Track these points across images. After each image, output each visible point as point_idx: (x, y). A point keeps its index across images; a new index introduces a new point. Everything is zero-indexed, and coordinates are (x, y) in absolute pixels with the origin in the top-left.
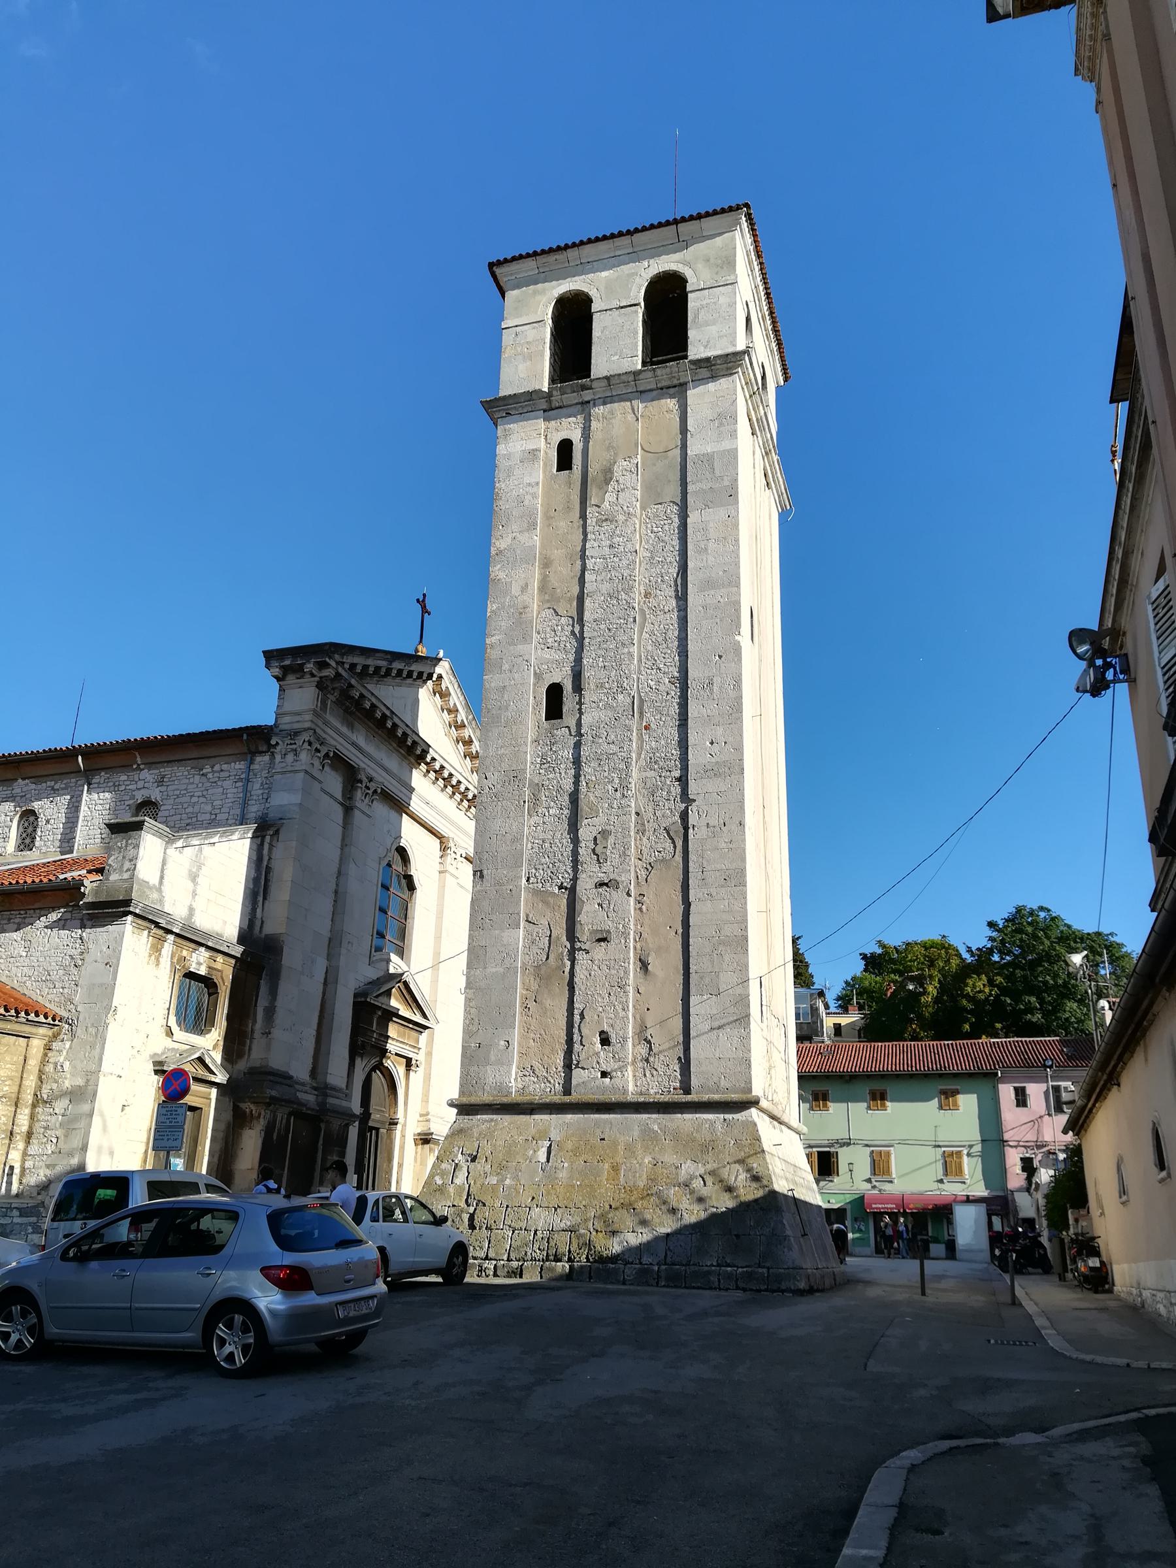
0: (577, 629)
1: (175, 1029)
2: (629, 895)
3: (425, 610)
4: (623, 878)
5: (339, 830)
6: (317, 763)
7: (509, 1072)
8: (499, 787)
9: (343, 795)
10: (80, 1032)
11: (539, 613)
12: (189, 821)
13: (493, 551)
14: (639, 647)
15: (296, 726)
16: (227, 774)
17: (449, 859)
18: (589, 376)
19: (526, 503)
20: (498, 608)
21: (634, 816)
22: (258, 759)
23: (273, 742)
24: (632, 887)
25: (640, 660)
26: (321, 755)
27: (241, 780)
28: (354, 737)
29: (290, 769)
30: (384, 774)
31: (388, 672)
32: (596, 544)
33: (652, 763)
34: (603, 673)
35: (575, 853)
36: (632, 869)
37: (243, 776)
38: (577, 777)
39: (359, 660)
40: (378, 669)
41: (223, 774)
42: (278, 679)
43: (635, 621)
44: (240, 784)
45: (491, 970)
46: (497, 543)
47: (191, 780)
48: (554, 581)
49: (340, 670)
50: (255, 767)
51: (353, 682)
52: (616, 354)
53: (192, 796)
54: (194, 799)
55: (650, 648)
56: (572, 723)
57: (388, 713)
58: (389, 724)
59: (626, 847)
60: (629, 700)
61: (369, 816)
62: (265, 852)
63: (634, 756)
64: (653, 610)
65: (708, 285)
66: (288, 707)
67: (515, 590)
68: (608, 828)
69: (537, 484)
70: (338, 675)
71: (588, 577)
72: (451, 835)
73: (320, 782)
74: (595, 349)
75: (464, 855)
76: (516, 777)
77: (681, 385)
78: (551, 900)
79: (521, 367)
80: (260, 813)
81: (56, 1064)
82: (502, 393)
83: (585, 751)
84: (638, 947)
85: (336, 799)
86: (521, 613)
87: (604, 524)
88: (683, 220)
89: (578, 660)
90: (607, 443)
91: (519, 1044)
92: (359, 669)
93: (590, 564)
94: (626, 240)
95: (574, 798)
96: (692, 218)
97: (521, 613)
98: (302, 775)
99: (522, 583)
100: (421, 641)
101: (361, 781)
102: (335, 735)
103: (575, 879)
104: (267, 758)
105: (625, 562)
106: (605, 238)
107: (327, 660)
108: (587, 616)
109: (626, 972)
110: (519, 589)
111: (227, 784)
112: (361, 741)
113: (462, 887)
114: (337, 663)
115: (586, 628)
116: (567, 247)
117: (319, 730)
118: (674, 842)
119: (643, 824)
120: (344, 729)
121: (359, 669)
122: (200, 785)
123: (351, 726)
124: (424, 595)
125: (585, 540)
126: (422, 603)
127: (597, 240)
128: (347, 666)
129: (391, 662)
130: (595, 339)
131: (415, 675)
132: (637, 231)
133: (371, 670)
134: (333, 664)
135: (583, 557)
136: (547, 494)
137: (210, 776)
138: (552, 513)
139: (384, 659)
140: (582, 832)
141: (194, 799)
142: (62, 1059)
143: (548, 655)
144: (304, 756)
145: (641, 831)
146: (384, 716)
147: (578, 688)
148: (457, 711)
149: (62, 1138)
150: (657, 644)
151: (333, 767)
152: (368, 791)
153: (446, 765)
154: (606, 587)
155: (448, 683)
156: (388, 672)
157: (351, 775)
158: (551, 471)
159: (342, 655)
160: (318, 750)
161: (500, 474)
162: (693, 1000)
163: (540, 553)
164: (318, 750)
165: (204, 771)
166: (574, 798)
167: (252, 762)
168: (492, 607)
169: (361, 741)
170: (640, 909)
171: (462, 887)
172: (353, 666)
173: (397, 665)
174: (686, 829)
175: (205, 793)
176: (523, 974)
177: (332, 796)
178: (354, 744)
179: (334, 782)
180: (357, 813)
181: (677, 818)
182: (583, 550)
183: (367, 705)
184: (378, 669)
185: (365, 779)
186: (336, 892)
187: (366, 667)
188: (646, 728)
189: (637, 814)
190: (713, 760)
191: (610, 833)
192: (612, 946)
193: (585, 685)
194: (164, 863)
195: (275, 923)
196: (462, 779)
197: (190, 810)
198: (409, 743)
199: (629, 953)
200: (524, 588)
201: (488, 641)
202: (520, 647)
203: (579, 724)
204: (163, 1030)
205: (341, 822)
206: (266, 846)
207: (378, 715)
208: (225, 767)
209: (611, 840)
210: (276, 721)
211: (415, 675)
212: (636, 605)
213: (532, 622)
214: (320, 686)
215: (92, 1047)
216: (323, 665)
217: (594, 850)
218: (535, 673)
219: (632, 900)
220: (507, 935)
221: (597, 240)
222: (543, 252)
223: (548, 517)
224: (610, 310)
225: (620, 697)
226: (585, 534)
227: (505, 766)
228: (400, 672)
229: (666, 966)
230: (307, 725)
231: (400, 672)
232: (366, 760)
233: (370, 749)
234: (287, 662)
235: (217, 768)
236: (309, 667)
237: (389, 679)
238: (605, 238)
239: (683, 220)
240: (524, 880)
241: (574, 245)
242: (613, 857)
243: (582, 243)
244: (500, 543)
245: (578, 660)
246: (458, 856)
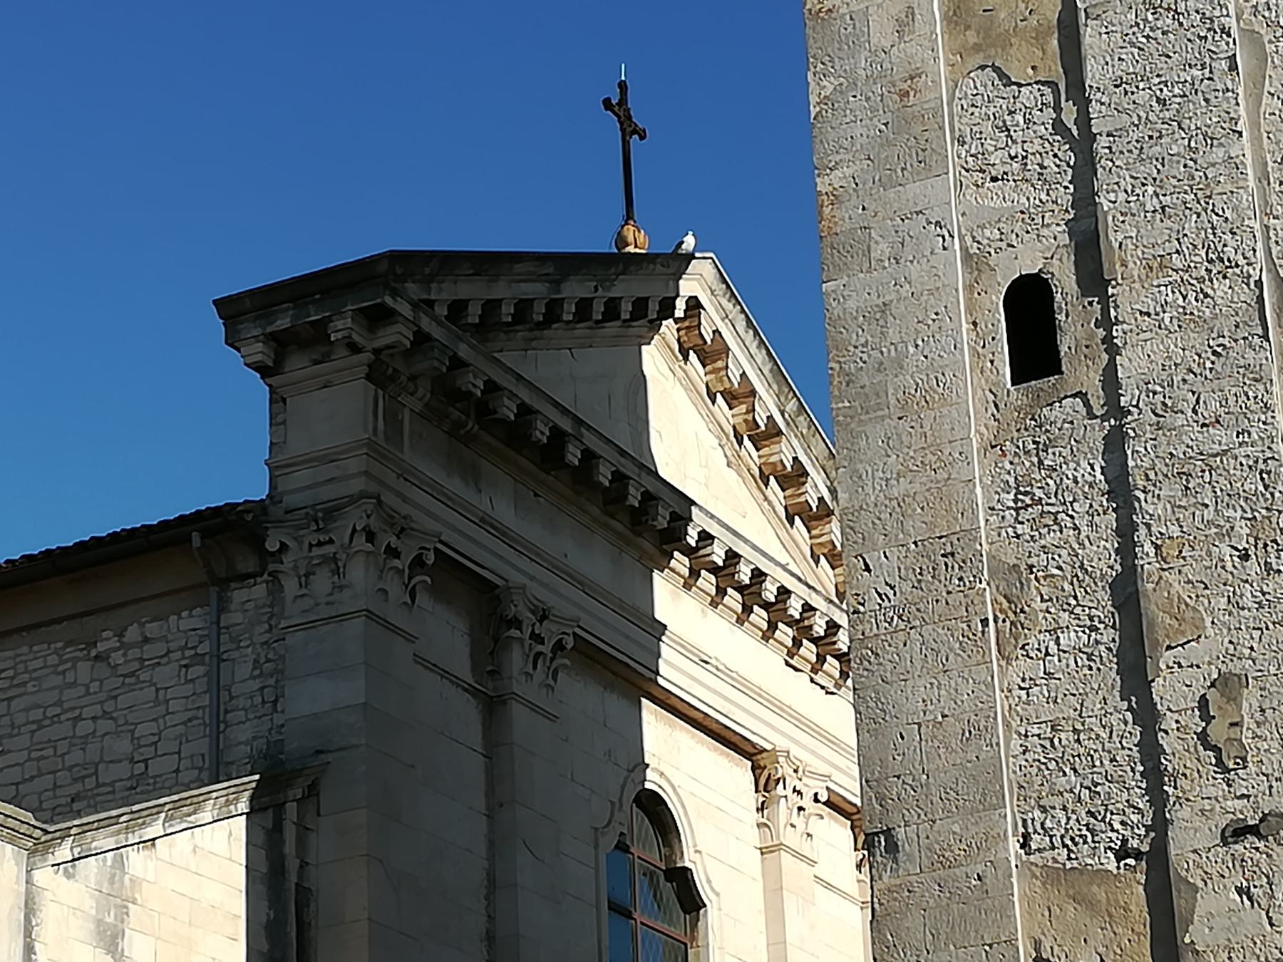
0: (1070, 115)
3: (629, 129)
6: (396, 589)
8: (907, 587)
9: (475, 667)
12: (78, 787)
14: (1256, 140)
15: (326, 493)
16: (160, 648)
17: (783, 811)
20: (838, 89)
22: (238, 596)
23: (272, 545)
25: (1264, 177)
26: (402, 563)
27: (198, 659)
28: (482, 502)
29: (325, 612)
30: (577, 595)
31: (553, 311)
34: (1161, 230)
35: (1150, 751)
37: (204, 648)
39: (473, 290)
40: (524, 306)
41: (150, 650)
42: (264, 371)
43: (1233, 67)
44: (198, 670)
47: (70, 677)
49: (426, 324)
50: (233, 617)
51: (464, 351)
53: (78, 719)
54: (84, 727)
56: (1092, 381)
57: (566, 425)
58: (573, 456)
60: (1247, 294)
61: (552, 718)
62: (290, 847)
66: (298, 445)
67: (881, 32)
68: (1235, 667)
70: (422, 338)
72: (781, 743)
73: (410, 638)
75: (823, 797)
78: (1100, 893)
80: (261, 744)
83: (1138, 458)
85: (456, 681)
89: (1085, 200)
92: (474, 314)
98: (359, 622)
99: (897, 9)
100: (629, 216)
101: (516, 623)
102: (438, 508)
103: (1160, 826)
104: (259, 591)
107: (388, 300)
108: (1093, 73)
110: (891, 26)
111: (165, 674)
112: (504, 512)
113: (829, 886)
114: (415, 305)
117: (388, 498)
120: (455, 485)
121: (474, 314)
122: (94, 686)
123: (473, 476)
124: (622, 86)
126: (619, 107)
128: (442, 311)
129: (556, 283)
131: (626, 309)
133: (507, 312)
134: (404, 308)
137: (117, 658)
139: (539, 278)
141: (84, 727)
143: (995, 199)
144: (357, 572)
146: (558, 436)
148: (753, 393)
151: (436, 591)
152: (540, 648)
153: (741, 549)
156: (553, 311)
159: (427, 282)
160: (393, 552)
164: (393, 552)
165: (101, 647)
167: (222, 609)
168: (819, 88)
169: (504, 512)
171: (829, 886)
172: (458, 308)
173: (575, 289)
175: (109, 707)
177: (445, 674)
178: (486, 522)
180: (517, 710)
183: (509, 410)
184: (524, 306)
185: (528, 617)
186: (490, 938)
187: (492, 306)
191: (1242, 680)
194: (30, 908)
196: (790, 583)
197: (76, 757)
198: (634, 500)
200: (906, 22)
201: (822, 185)
202: (913, 189)
203: (1111, 381)
205: (476, 739)
206: (290, 832)
207: (541, 433)
208: (153, 629)
209: (1250, 699)
210: (272, 486)
211: (626, 309)
212: (1232, 23)
213: (938, 112)
214: (378, 375)
216: (378, 317)
217: (1203, 736)
218: (967, 256)
225: (1221, 289)
227: (915, 528)
228: (584, 307)
230: (356, 486)
231: (584, 307)
232: (523, 563)
233: (531, 531)
234: (283, 323)
235: (132, 634)
236: (341, 327)
237: (556, 331)
240: (1014, 845)
245: (1085, 200)
246: (807, 802)
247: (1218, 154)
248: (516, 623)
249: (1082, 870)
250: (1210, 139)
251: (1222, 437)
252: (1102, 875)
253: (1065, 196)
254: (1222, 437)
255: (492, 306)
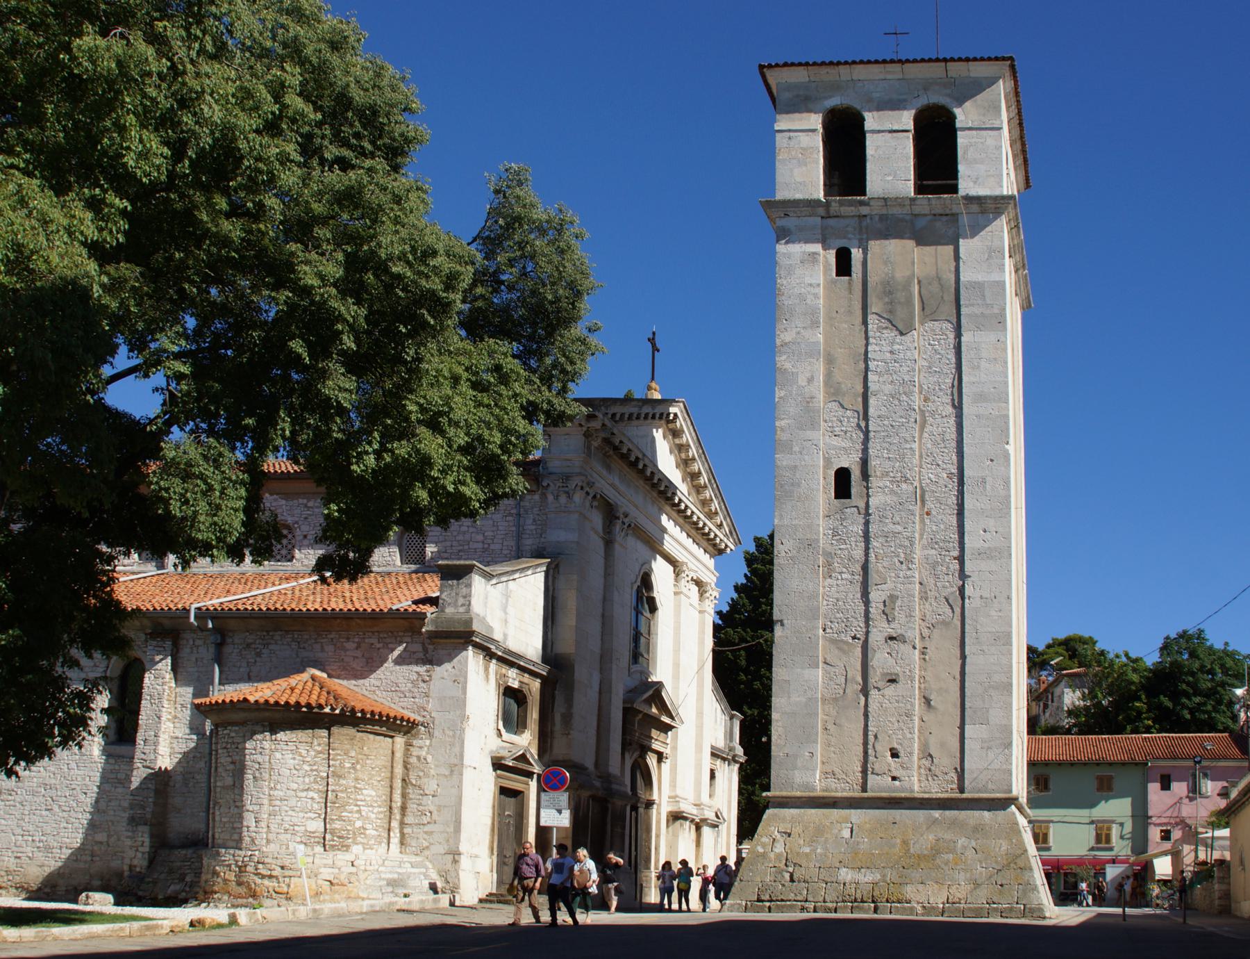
0: (863, 424)
1: (503, 731)
2: (914, 648)
4: (909, 634)
5: (602, 561)
7: (815, 775)
9: (604, 529)
10: (436, 733)
11: (825, 403)
13: (778, 342)
18: (863, 192)
19: (808, 301)
20: (785, 395)
21: (917, 586)
24: (917, 641)
25: (921, 456)
32: (877, 348)
33: (933, 543)
34: (887, 464)
35: (867, 613)
36: (917, 627)
38: (867, 549)
39: (618, 409)
45: (795, 698)
46: (782, 336)
48: (838, 376)
52: (890, 175)
55: (929, 446)
56: (862, 505)
57: (640, 456)
58: (641, 466)
59: (911, 609)
60: (911, 488)
63: (917, 535)
64: (933, 414)
65: (976, 125)
67: (802, 381)
68: (895, 593)
69: (819, 285)
71: (871, 376)
74: (870, 166)
76: (811, 544)
77: (953, 215)
78: (846, 647)
79: (796, 172)
81: (419, 758)
82: (780, 196)
83: (873, 528)
84: (923, 686)
86: (808, 402)
87: (885, 331)
88: (952, 60)
89: (865, 450)
90: (885, 257)
91: (822, 755)
93: (872, 365)
94: (897, 67)
95: (865, 568)
96: (960, 60)
97: (808, 402)
100: (653, 379)
101: (618, 518)
105: (906, 369)
106: (876, 62)
108: (871, 411)
109: (912, 705)
110: (805, 380)
112: (617, 482)
115: (870, 422)
116: (839, 63)
118: (952, 608)
119: (926, 592)
120: (604, 472)
123: (609, 468)
125: (867, 345)
126: (652, 341)
127: (869, 62)
129: (641, 407)
130: (869, 156)
132: (908, 61)
135: (866, 359)
136: (828, 297)
138: (834, 315)
139: (635, 406)
140: (873, 596)
142: (424, 753)
143: (835, 442)
145: (924, 598)
146: (637, 458)
147: (865, 475)
149: (435, 813)
150: (935, 443)
154: (888, 388)
155: (682, 422)
157: (610, 513)
158: (831, 275)
161: (781, 272)
162: (967, 727)
163: (824, 349)
166: (865, 568)
168: (779, 393)
170: (924, 659)
173: (647, 409)
174: (963, 598)
176: (823, 704)
179: (597, 519)
181: (955, 589)
182: (866, 352)
184: (631, 416)
187: (622, 415)
188: (928, 514)
189: (921, 584)
190: (986, 545)
192: (900, 686)
193: (871, 472)
195: (566, 645)
199: (914, 691)
201: (777, 424)
204: (495, 731)
207: (633, 459)
209: (899, 603)
212: (917, 408)
213: (819, 411)
215: (452, 745)
217: (884, 612)
218: (824, 458)
219: (917, 652)
220: (808, 673)
221: (869, 62)
222: (815, 64)
223: (830, 319)
224: (883, 131)
226: (867, 338)
227: (799, 535)
229: (947, 703)
231: (647, 415)
232: (621, 498)
233: (622, 488)
237: (635, 422)
238: (876, 62)
239: (952, 60)
240: (821, 631)
241: (846, 63)
242: (900, 616)
243: (854, 62)
244: (785, 335)
245: (865, 450)
247: (908, 446)
248: (618, 518)
249: (842, 641)
250: (906, 441)
251: (899, 528)
252: (846, 643)
253: (859, 447)
254: (899, 528)
255: (622, 415)
